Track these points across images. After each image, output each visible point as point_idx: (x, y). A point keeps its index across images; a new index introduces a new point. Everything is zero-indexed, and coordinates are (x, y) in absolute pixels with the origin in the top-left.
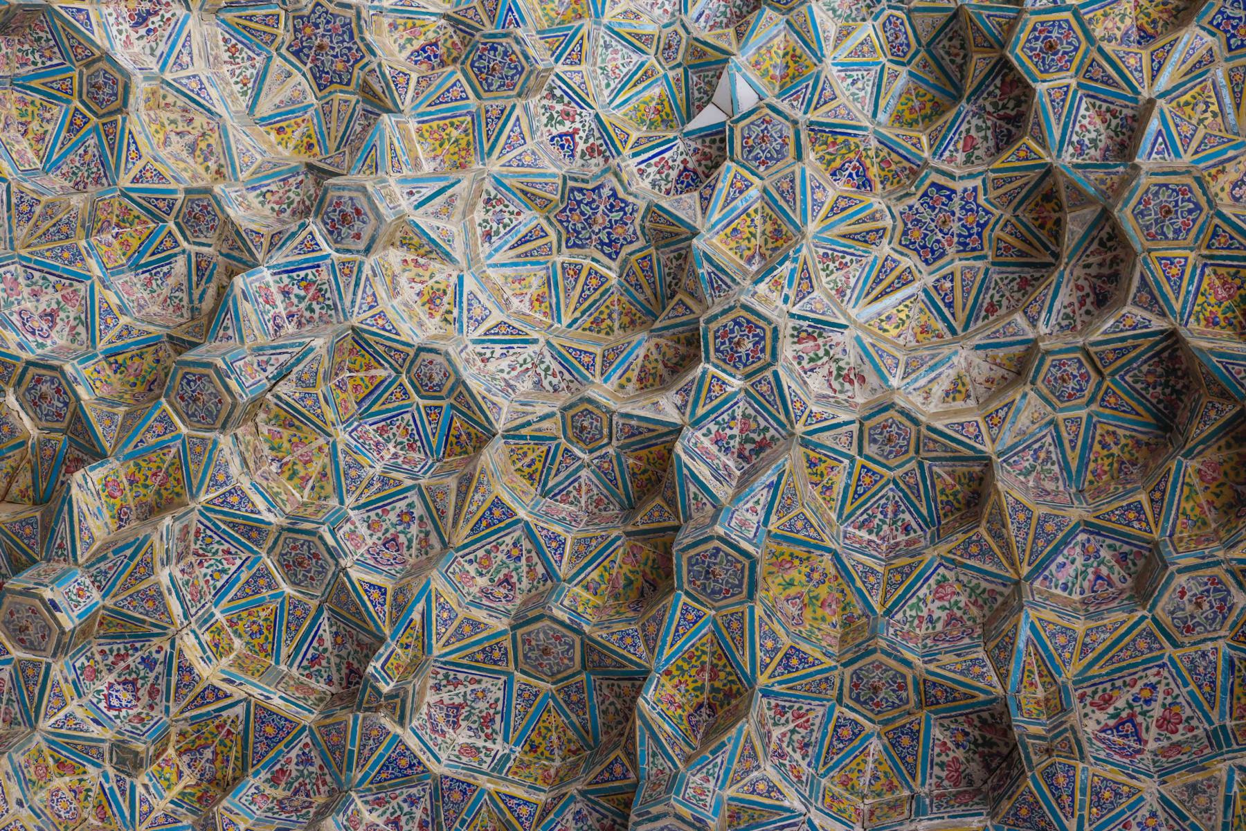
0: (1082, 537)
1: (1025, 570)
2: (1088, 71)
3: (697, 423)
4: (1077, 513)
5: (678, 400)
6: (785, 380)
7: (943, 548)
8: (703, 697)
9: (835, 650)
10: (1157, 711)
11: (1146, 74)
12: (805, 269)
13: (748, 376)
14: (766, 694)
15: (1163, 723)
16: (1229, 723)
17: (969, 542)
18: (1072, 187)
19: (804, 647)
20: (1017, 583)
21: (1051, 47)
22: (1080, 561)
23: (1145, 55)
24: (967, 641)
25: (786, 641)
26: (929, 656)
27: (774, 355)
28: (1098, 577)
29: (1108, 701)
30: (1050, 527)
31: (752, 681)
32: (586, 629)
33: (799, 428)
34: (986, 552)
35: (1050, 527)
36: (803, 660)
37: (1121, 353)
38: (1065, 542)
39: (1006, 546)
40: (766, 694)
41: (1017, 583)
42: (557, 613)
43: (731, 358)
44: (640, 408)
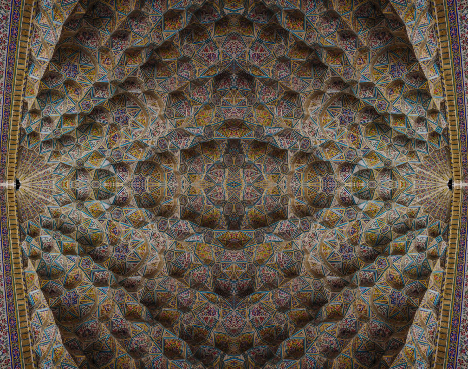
0: (289, 296)
1: (280, 288)
2: (379, 271)
3: (289, 221)
4: (292, 293)
5: (293, 216)
6: (302, 235)
7: (280, 272)
8: (240, 240)
9: (256, 259)
10: (263, 316)
11: (381, 282)
12: (325, 231)
13: (300, 228)
14: (243, 251)
15: (261, 318)
16: (264, 329)
17: (282, 277)
18: (353, 275)
19: (254, 255)
20: (277, 287)
21: (381, 264)
22: (285, 296)
23: (385, 281)
24: (265, 281)
25: (253, 251)
26: (260, 276)
27: (305, 232)
28: (283, 300)
29: (261, 308)
30: (288, 290)
31: (244, 248)
32: (245, 215)
33: (294, 240)
34: (281, 280)
35: (288, 290)
36: (251, 255)
37: (323, 294)
38: (287, 293)
39: (283, 283)
40: (243, 251)
41: (277, 287)
42: (246, 209)
43: (302, 224)
44: (289, 210)
